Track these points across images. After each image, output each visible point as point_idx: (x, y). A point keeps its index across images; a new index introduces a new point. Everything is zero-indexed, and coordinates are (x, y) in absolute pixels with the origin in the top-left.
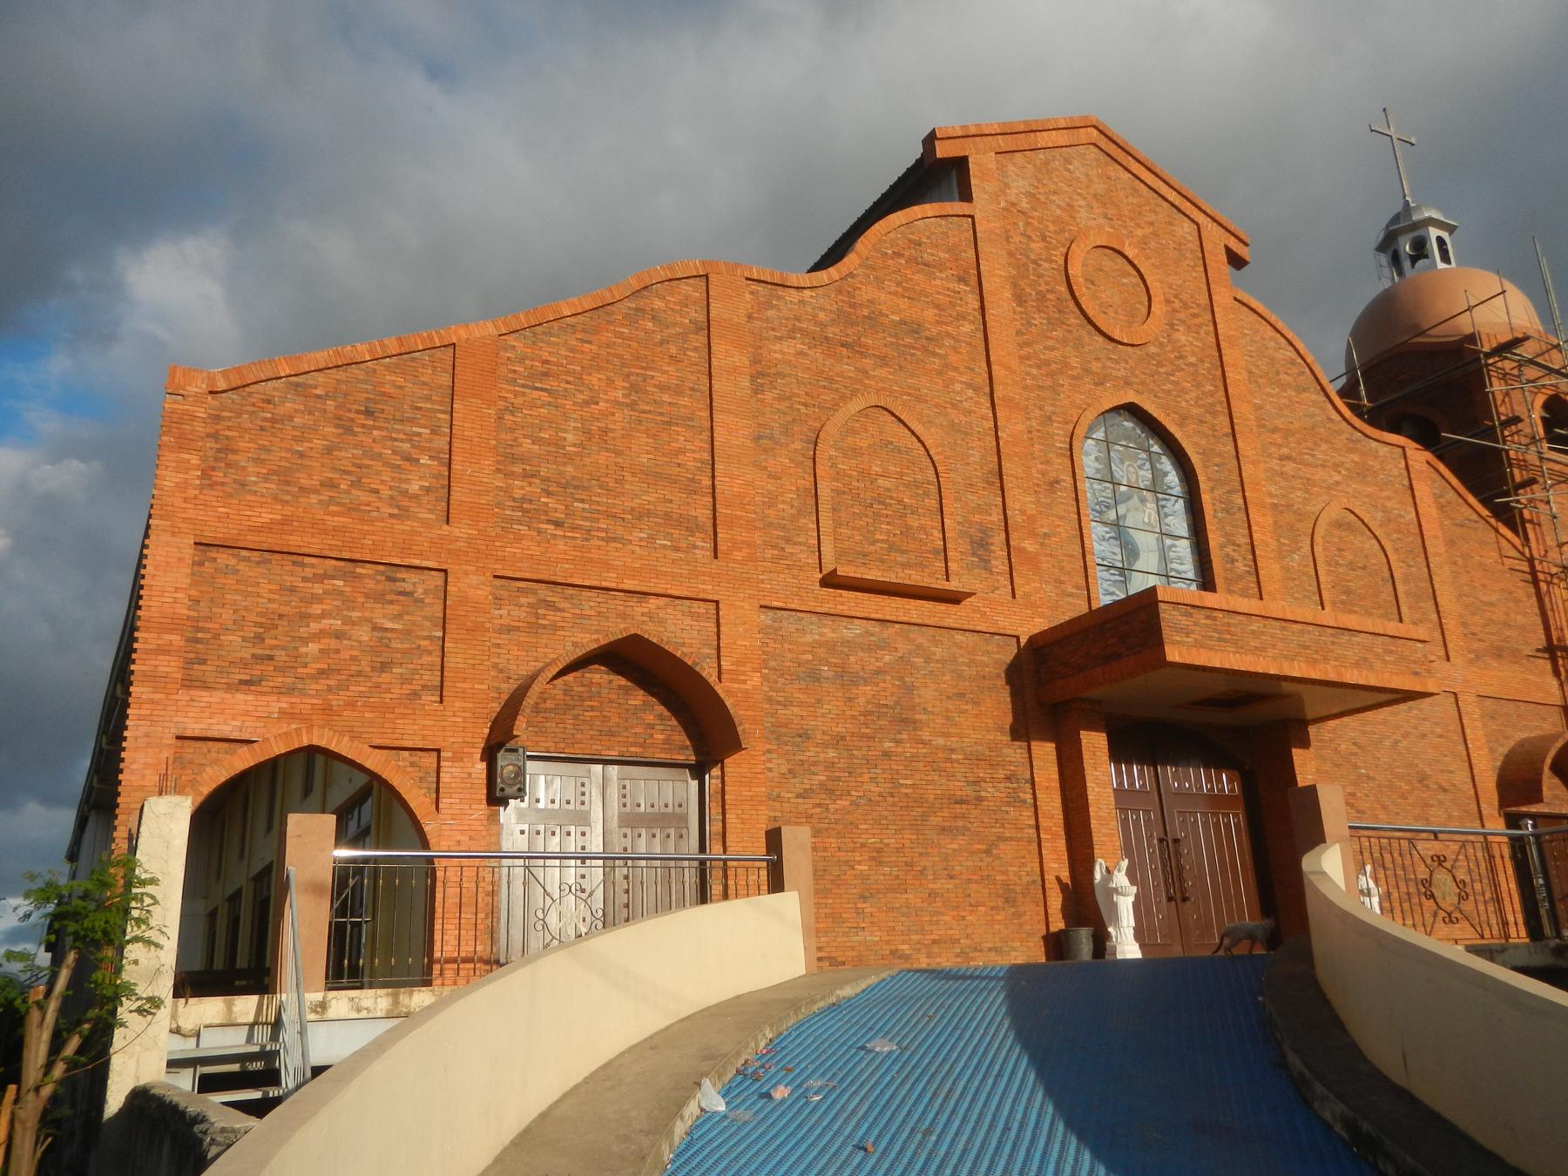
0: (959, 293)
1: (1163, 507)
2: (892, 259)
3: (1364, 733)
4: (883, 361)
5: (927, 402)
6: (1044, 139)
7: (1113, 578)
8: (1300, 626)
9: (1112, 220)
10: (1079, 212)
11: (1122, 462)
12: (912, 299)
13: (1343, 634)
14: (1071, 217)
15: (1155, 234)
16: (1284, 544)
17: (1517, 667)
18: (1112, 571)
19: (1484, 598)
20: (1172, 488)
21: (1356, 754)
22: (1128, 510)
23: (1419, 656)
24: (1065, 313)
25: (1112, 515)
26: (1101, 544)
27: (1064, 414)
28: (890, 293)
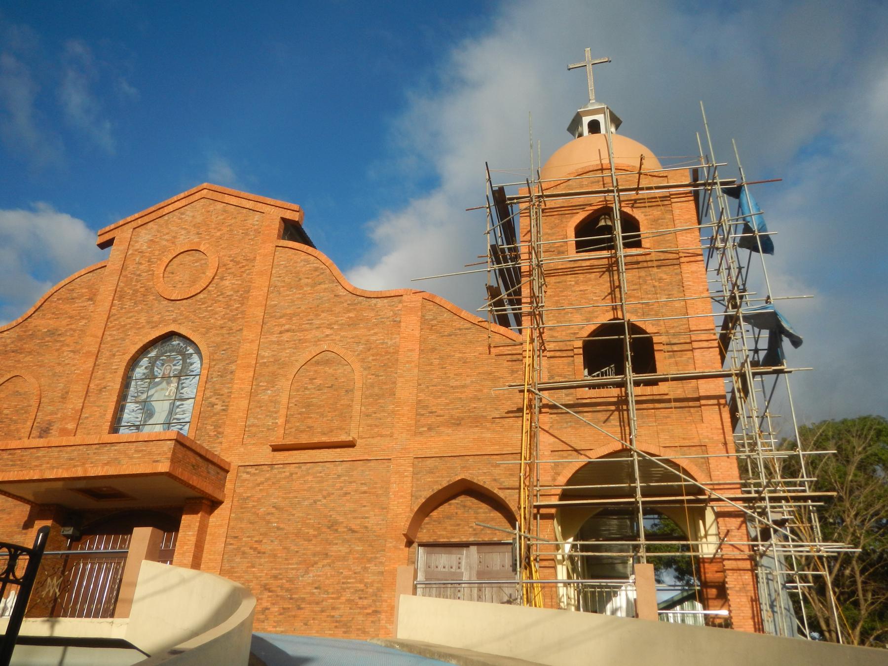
0: (85, 306)
1: (182, 383)
2: (55, 302)
3: (288, 498)
4: (30, 353)
5: (44, 366)
6: (166, 210)
7: (130, 432)
8: (74, 448)
9: (201, 234)
10: (179, 238)
11: (163, 365)
12: (58, 318)
13: (106, 446)
14: (173, 243)
15: (231, 230)
16: (262, 386)
17: (476, 430)
18: (132, 428)
19: (458, 383)
20: (193, 371)
21: (272, 514)
22: (156, 391)
23: (165, 449)
24: (147, 295)
25: (144, 396)
26: (131, 413)
27: (124, 350)
28: (47, 319)
